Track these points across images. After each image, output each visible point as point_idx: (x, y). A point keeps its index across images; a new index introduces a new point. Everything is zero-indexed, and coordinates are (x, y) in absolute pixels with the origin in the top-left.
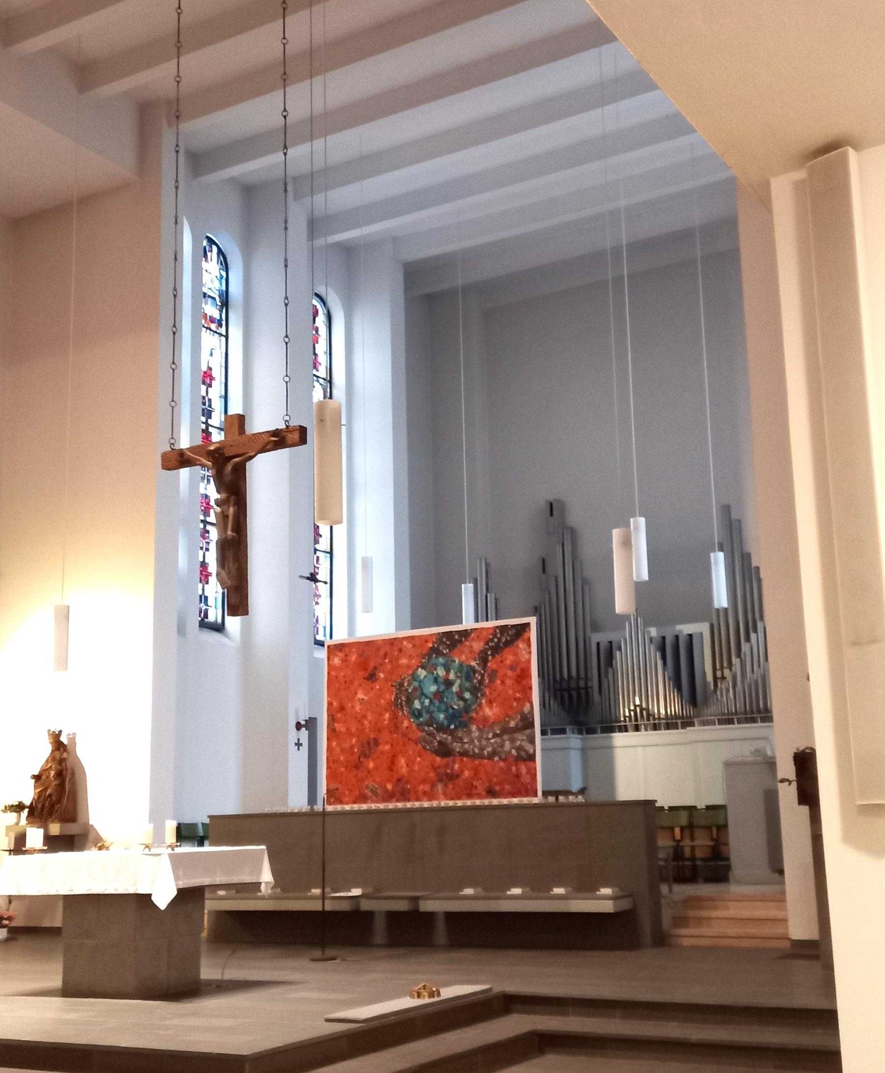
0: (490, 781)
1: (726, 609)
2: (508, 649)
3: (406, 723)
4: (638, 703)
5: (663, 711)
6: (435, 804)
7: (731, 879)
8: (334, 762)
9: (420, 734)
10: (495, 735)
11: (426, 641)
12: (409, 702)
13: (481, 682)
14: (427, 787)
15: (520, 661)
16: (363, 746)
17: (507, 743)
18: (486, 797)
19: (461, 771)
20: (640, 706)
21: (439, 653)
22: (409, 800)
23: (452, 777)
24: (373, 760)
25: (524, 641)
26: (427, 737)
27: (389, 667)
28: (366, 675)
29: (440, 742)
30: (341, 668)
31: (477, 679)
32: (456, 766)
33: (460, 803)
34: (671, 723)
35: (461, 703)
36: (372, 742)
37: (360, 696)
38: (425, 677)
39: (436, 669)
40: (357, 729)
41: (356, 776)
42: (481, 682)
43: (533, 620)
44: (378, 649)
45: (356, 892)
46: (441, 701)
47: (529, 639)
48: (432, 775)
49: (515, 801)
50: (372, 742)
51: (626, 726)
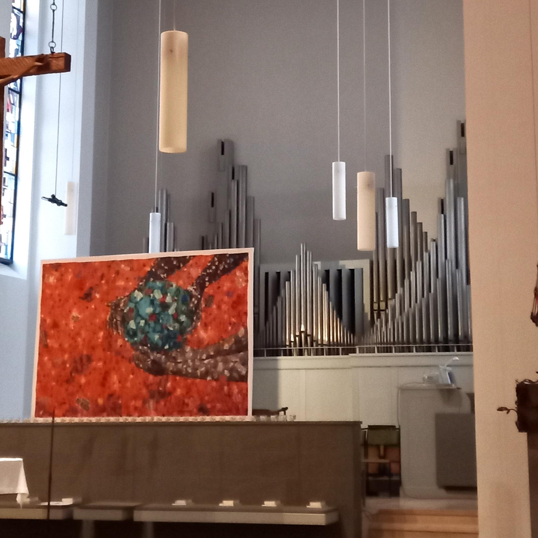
0: (202, 399)
2: (223, 277)
3: (120, 342)
4: (303, 329)
5: (326, 338)
6: (148, 419)
8: (44, 376)
11: (144, 265)
12: (125, 321)
13: (197, 306)
14: (139, 403)
16: (75, 362)
18: (196, 414)
19: (174, 389)
20: (305, 332)
21: (157, 277)
23: (164, 395)
24: (85, 376)
25: (241, 270)
27: (105, 288)
28: (82, 294)
29: (154, 362)
30: (56, 288)
31: (193, 303)
32: (169, 385)
33: (172, 419)
34: (332, 350)
35: (177, 325)
36: (85, 360)
37: (75, 313)
38: (142, 299)
39: (152, 292)
40: (70, 346)
42: (197, 306)
43: (251, 251)
44: (95, 270)
45: (67, 501)
46: (157, 321)
47: (246, 268)
48: (144, 391)
49: (228, 418)
51: (290, 350)
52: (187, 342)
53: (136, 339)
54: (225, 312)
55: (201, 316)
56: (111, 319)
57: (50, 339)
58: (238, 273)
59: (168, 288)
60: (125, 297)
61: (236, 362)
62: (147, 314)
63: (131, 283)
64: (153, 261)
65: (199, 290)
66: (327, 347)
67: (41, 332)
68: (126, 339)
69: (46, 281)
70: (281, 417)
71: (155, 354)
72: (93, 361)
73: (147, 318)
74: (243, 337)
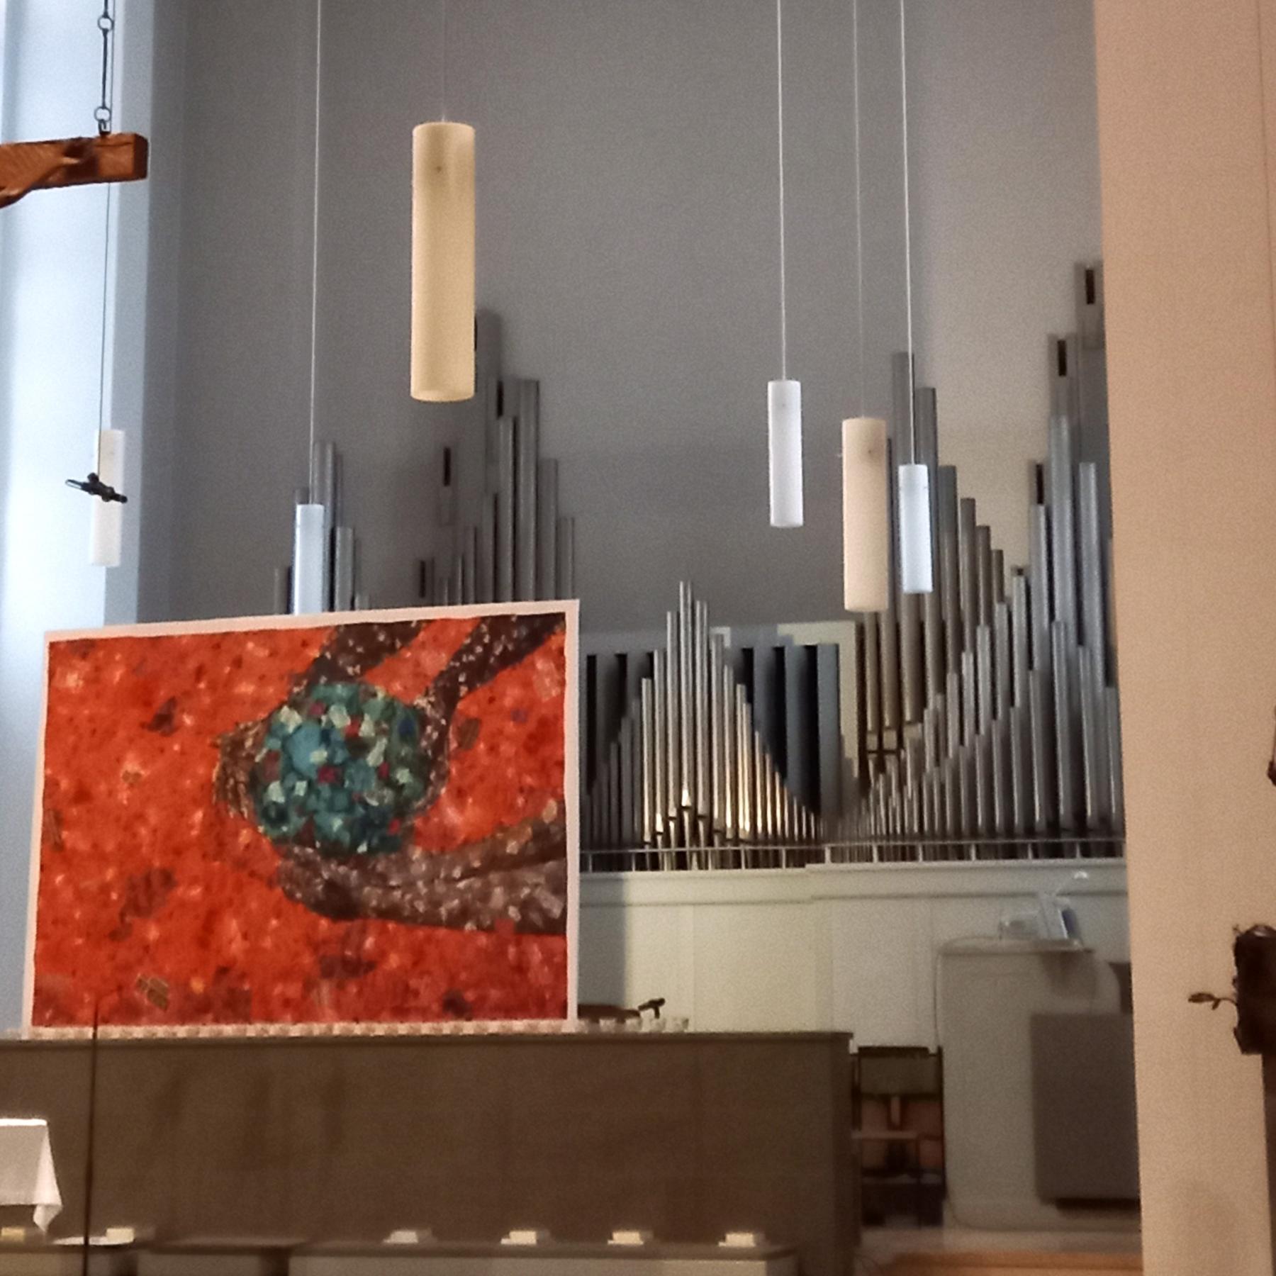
0: (452, 978)
1: (918, 598)
2: (505, 673)
3: (245, 836)
4: (686, 801)
5: (745, 824)
7: (947, 1215)
9: (279, 863)
10: (469, 873)
11: (305, 644)
12: (257, 784)
14: (293, 990)
15: (534, 703)
16: (133, 887)
17: (498, 891)
18: (439, 1017)
19: (383, 954)
20: (693, 809)
21: (336, 674)
22: (248, 1019)
23: (359, 967)
24: (158, 921)
25: (547, 654)
26: (298, 871)
27: (207, 700)
28: (147, 717)
29: (331, 885)
30: (82, 700)
31: (430, 736)
32: (369, 943)
33: (380, 1029)
34: (761, 853)
35: (388, 794)
36: (156, 881)
37: (131, 765)
38: (299, 728)
39: (326, 711)
40: (120, 847)
41: (112, 957)
43: (570, 608)
44: (183, 657)
46: (337, 784)
47: (561, 651)
48: (307, 959)
50: (156, 881)
52: (414, 835)
53: (285, 829)
54: (508, 760)
55: (449, 772)
56: (224, 778)
57: (68, 829)
58: (540, 665)
59: (365, 701)
60: (255, 724)
61: (537, 885)
62: (313, 765)
63: (271, 690)
64: (328, 632)
65: (443, 704)
66: (748, 848)
67: (46, 811)
68: (261, 829)
69: (56, 683)
70: (647, 1024)
71: (333, 866)
72: (176, 885)
73: (314, 776)
74: (552, 823)
